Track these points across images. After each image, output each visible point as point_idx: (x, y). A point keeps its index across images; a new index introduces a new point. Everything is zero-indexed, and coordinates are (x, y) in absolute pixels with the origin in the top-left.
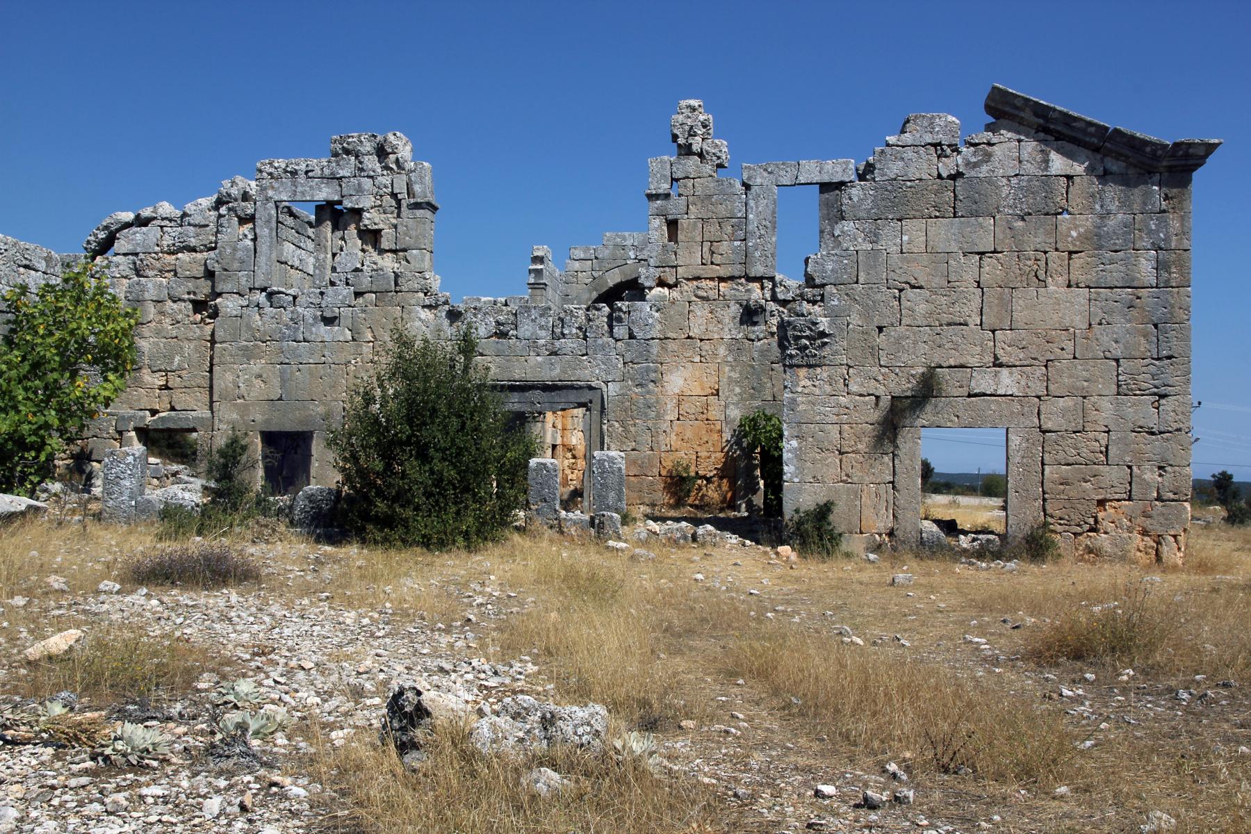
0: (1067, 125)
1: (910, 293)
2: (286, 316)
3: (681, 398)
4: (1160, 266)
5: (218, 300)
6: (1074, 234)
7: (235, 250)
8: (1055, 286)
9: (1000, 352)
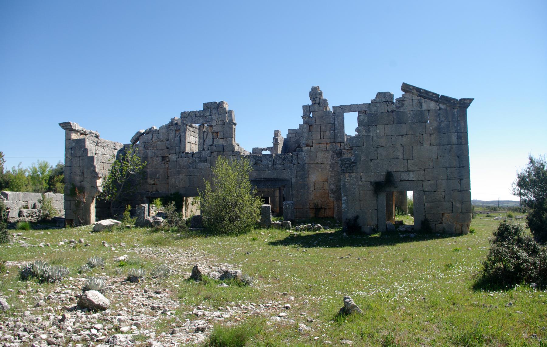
0: (427, 94)
1: (380, 149)
2: (190, 160)
3: (315, 183)
4: (459, 138)
6: (431, 128)
7: (174, 140)
8: (426, 145)
9: (409, 167)
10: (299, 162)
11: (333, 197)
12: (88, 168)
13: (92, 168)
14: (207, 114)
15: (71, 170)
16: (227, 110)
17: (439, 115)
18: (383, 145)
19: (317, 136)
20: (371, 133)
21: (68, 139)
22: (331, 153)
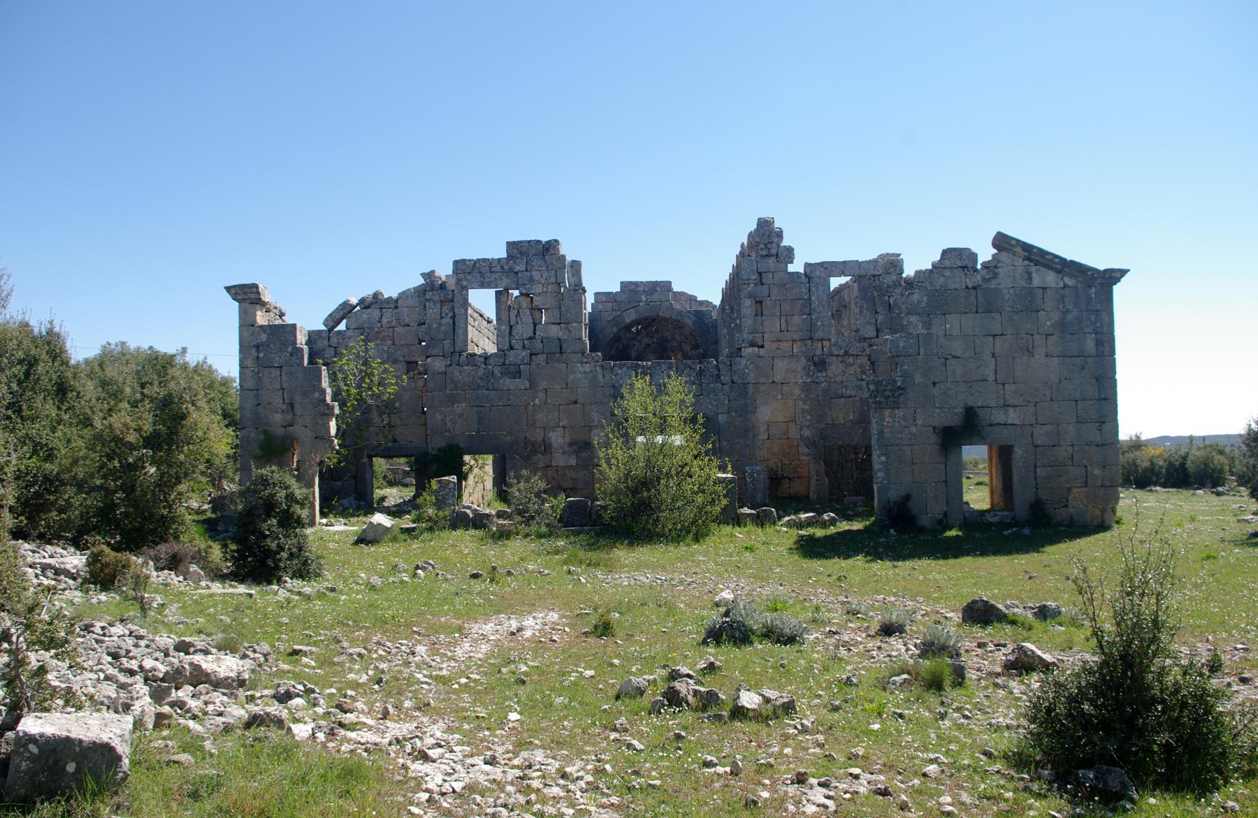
1: (953, 361)
2: (481, 372)
3: (769, 424)
4: (1099, 343)
5: (429, 360)
7: (440, 325)
8: (1039, 356)
9: (1008, 397)
10: (735, 378)
11: (808, 455)
12: (305, 394)
13: (317, 395)
14: (520, 267)
15: (257, 397)
16: (569, 259)
17: (1063, 297)
18: (959, 354)
19: (772, 325)
20: (934, 330)
21: (247, 324)
22: (803, 360)
